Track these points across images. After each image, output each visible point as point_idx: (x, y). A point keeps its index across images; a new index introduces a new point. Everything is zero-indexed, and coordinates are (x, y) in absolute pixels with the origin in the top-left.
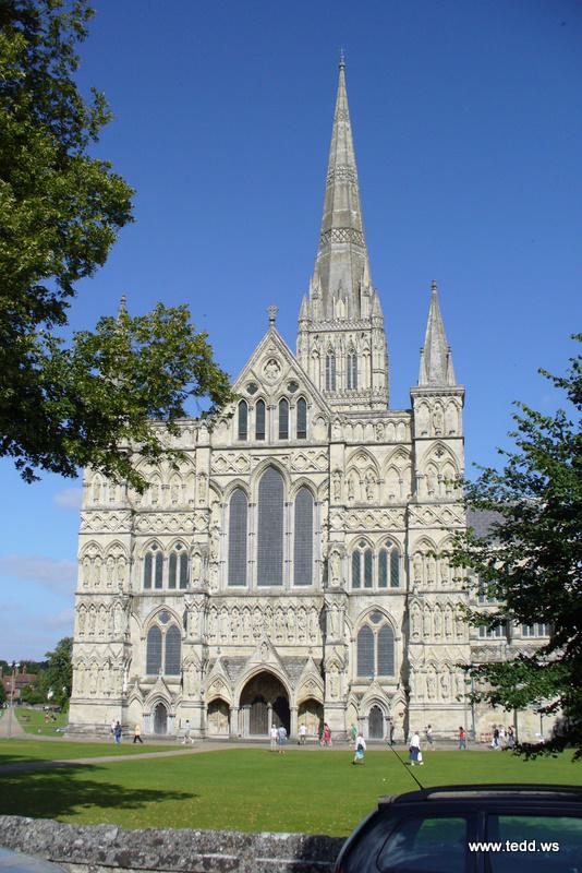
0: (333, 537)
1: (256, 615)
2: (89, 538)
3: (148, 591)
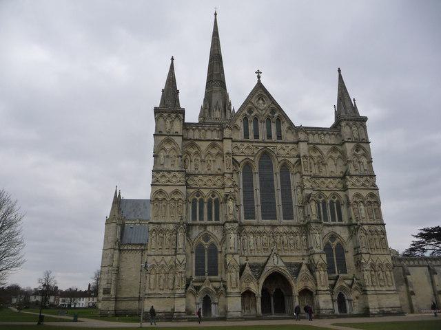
1: (264, 237)
2: (158, 188)
3: (195, 222)
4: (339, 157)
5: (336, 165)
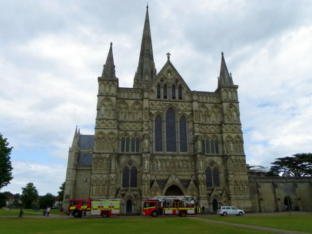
0: (196, 134)
1: (168, 162)
2: (100, 130)
3: (123, 153)
4: (219, 111)
5: (216, 116)
